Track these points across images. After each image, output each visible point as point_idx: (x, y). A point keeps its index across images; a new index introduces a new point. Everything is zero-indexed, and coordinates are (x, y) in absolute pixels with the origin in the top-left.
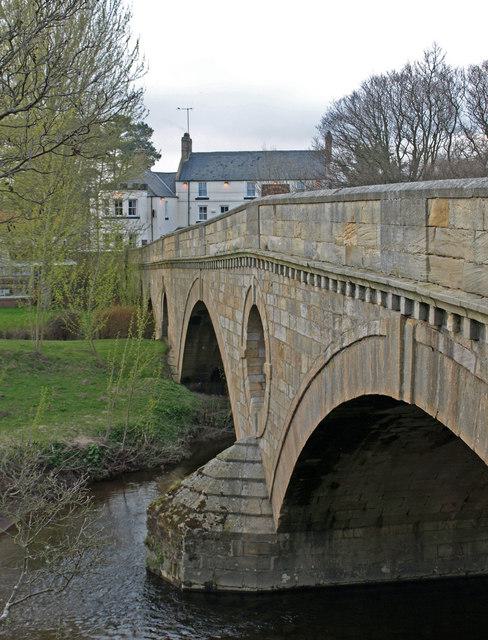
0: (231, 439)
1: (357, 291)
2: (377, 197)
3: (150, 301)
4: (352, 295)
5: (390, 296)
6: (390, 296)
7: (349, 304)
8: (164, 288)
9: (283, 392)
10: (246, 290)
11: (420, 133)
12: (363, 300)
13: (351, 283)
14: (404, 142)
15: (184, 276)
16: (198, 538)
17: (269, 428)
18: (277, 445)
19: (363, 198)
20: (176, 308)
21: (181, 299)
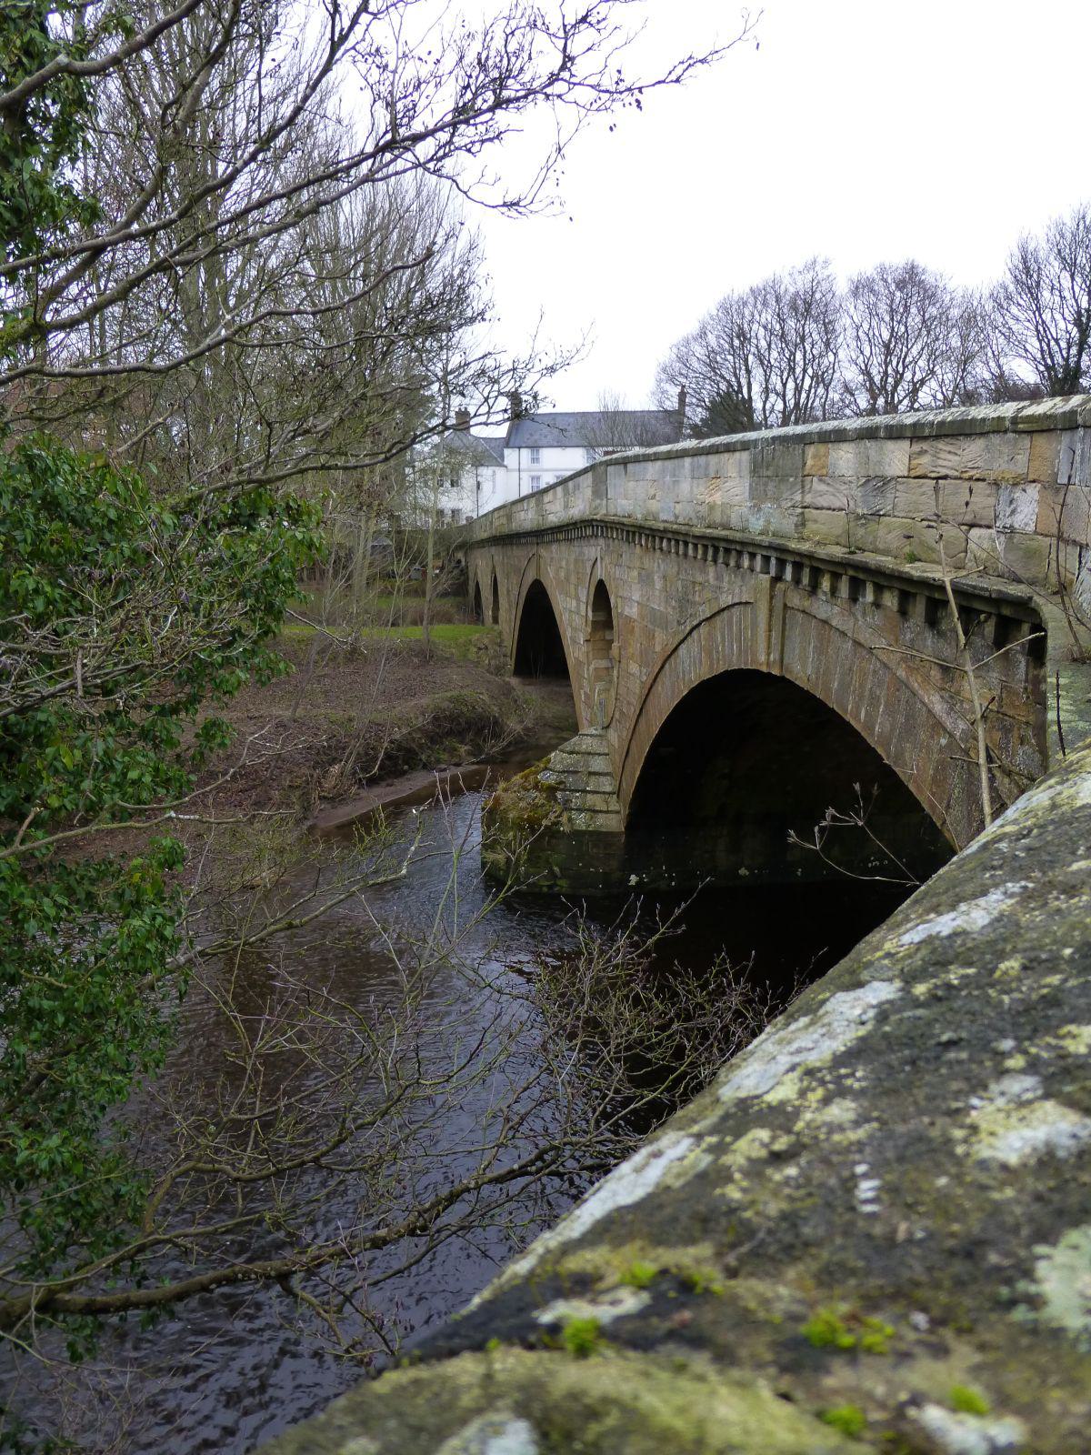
0: (574, 729)
1: (721, 554)
2: (745, 446)
3: (477, 584)
4: (715, 561)
5: (759, 558)
6: (759, 558)
7: (711, 570)
8: (494, 567)
9: (636, 673)
10: (591, 563)
11: (791, 385)
12: (727, 565)
13: (713, 546)
14: (773, 397)
15: (519, 554)
16: (544, 838)
17: (617, 716)
18: (626, 734)
19: (729, 448)
20: (508, 591)
21: (515, 580)
